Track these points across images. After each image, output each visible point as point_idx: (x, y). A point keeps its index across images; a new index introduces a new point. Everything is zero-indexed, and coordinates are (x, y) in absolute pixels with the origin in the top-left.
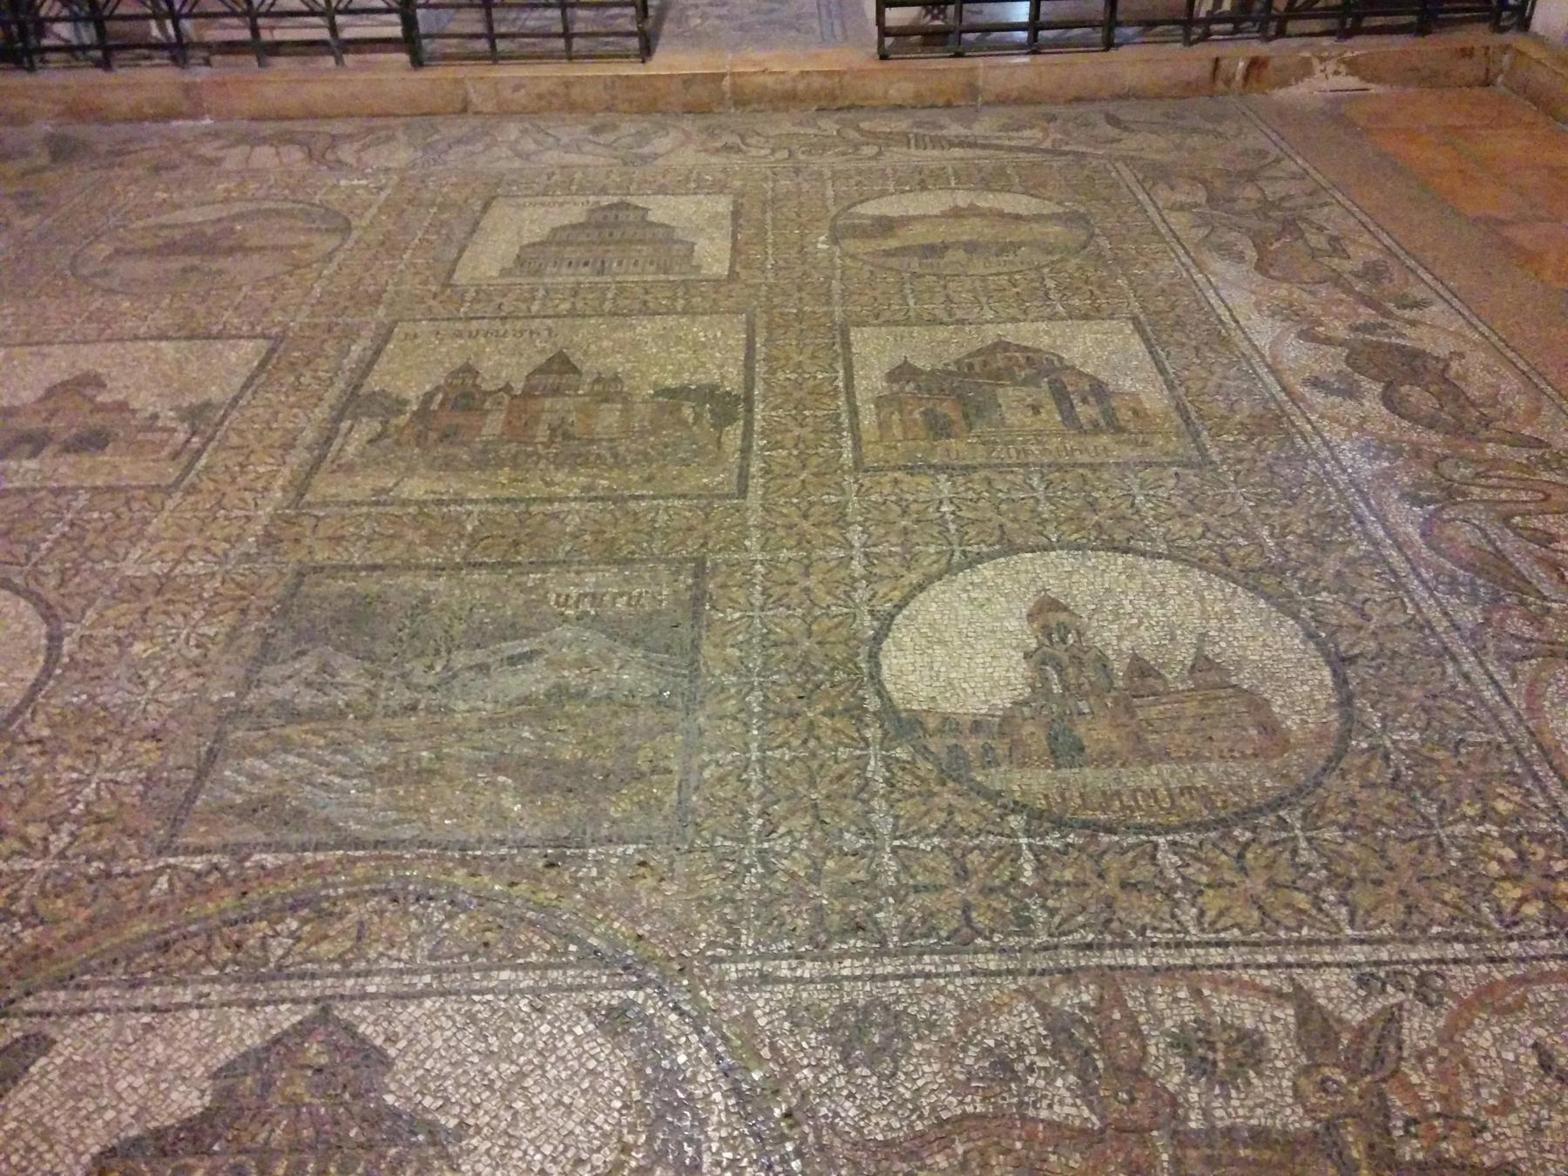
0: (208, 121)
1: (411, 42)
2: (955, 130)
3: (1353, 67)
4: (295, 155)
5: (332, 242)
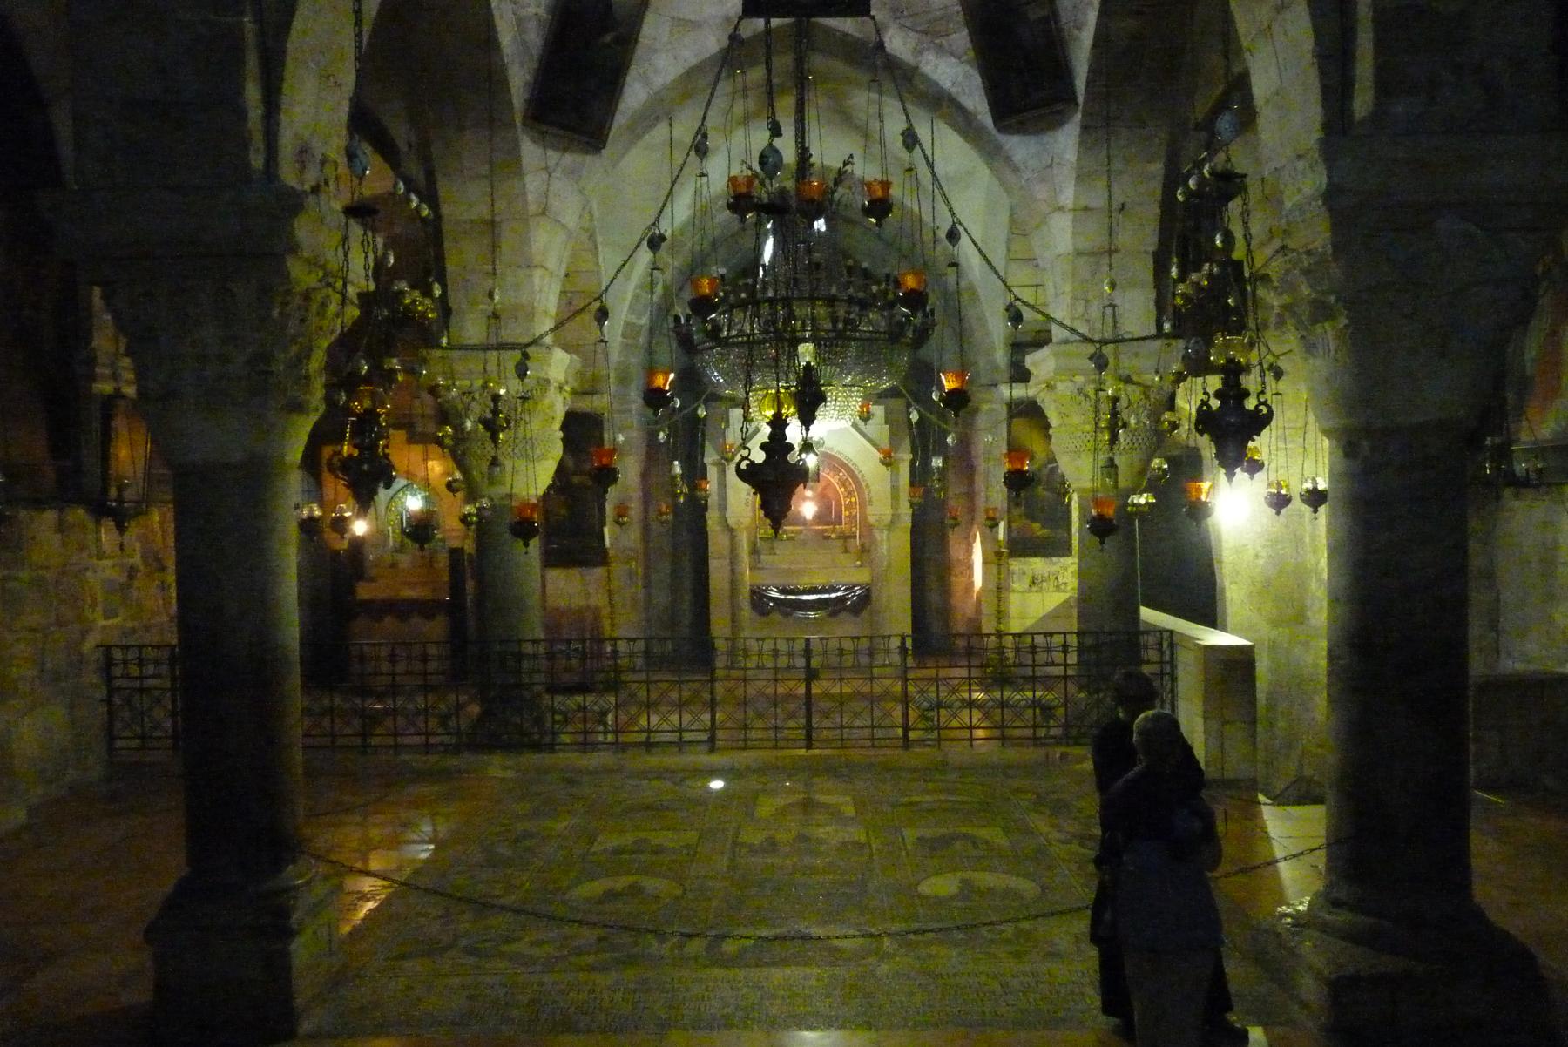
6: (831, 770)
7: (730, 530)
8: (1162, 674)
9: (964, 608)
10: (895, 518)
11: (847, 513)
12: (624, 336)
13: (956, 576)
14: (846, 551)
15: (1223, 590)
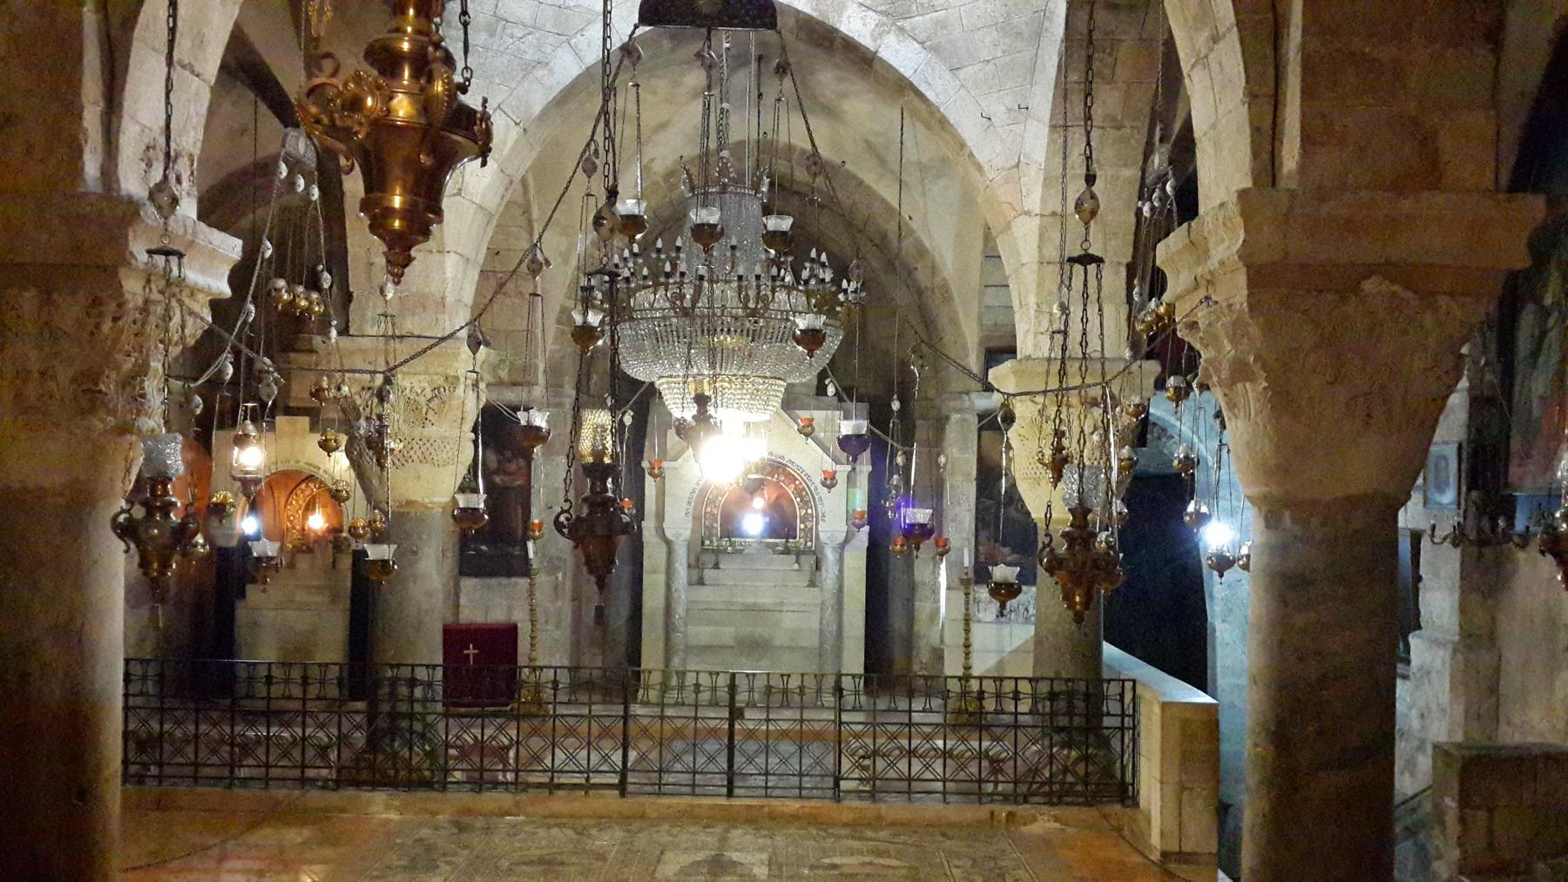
0: (522, 818)
1: (622, 787)
2: (869, 834)
3: (1057, 819)
4: (570, 832)
5: (600, 864)
6: (752, 819)
7: (668, 543)
8: (1122, 729)
9: (928, 636)
11: (802, 526)
13: (920, 601)
15: (1214, 630)
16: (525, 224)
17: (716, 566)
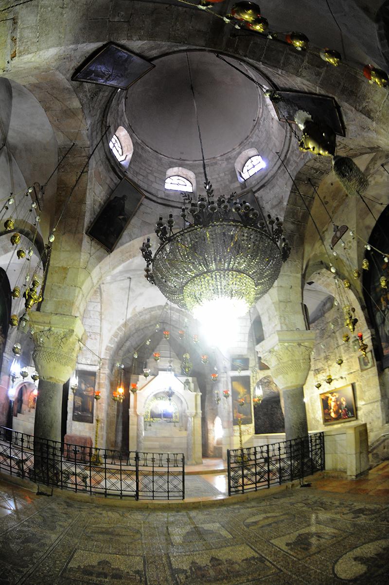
7: (138, 416)
10: (196, 413)
12: (106, 350)
14: (175, 426)
16: (100, 318)
17: (150, 425)
